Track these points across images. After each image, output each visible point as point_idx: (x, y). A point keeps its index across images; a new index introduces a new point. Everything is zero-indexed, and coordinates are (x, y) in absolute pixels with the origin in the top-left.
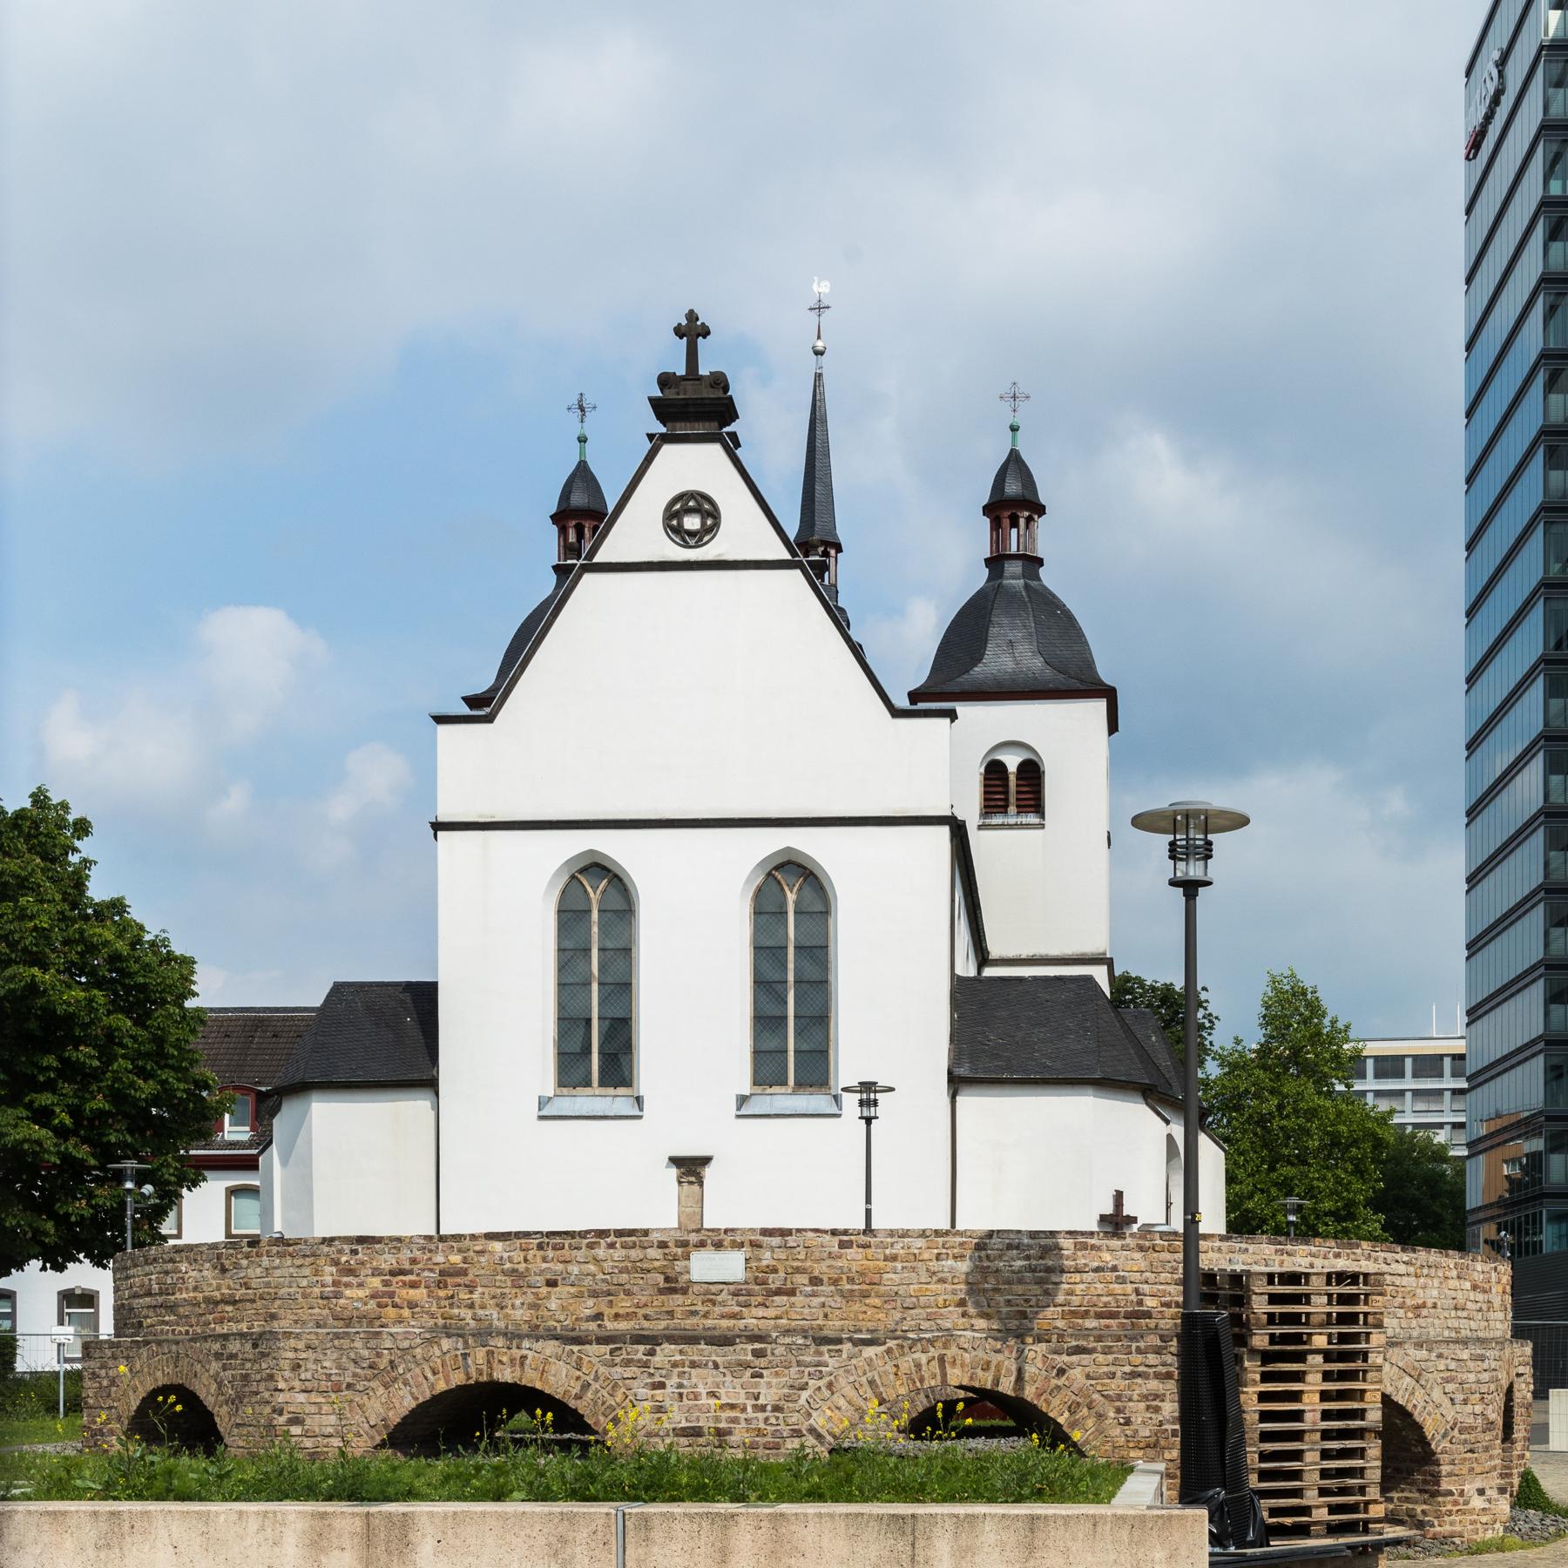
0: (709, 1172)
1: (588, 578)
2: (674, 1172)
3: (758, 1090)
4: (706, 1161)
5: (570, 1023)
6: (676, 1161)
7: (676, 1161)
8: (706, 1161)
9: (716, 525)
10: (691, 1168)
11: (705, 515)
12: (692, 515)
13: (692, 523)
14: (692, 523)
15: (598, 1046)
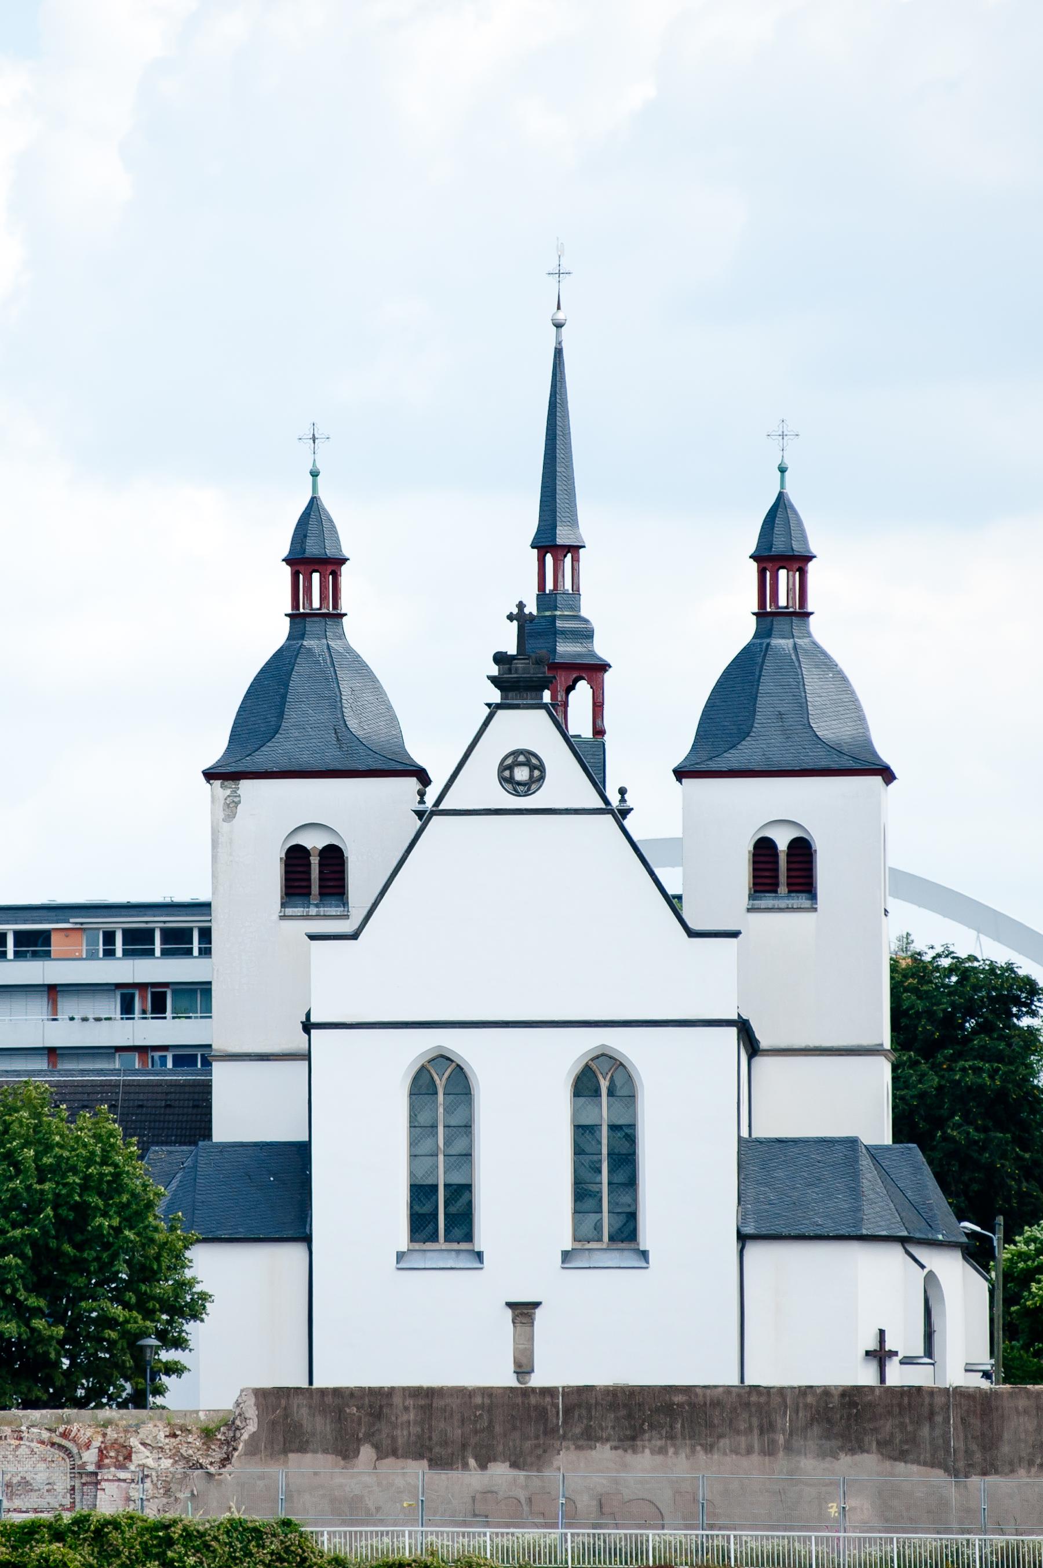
0: (538, 1312)
1: (435, 819)
2: (509, 1313)
3: (578, 1246)
4: (537, 1305)
5: (421, 1193)
6: (510, 1305)
7: (510, 1305)
8: (537, 1305)
9: (542, 778)
10: (523, 1312)
11: (532, 768)
12: (522, 772)
13: (521, 774)
14: (521, 774)
15: (441, 1214)
